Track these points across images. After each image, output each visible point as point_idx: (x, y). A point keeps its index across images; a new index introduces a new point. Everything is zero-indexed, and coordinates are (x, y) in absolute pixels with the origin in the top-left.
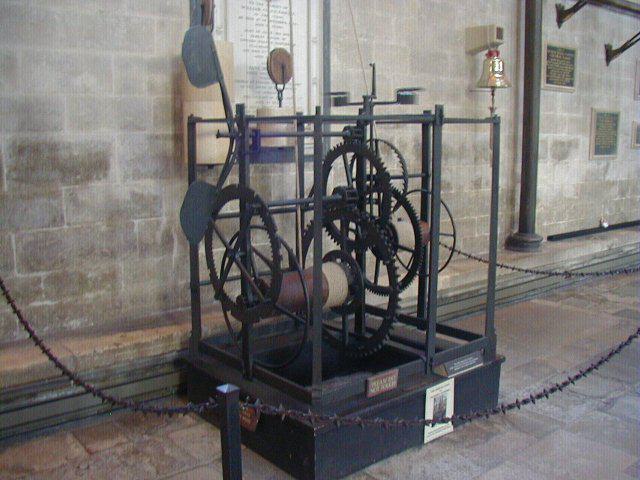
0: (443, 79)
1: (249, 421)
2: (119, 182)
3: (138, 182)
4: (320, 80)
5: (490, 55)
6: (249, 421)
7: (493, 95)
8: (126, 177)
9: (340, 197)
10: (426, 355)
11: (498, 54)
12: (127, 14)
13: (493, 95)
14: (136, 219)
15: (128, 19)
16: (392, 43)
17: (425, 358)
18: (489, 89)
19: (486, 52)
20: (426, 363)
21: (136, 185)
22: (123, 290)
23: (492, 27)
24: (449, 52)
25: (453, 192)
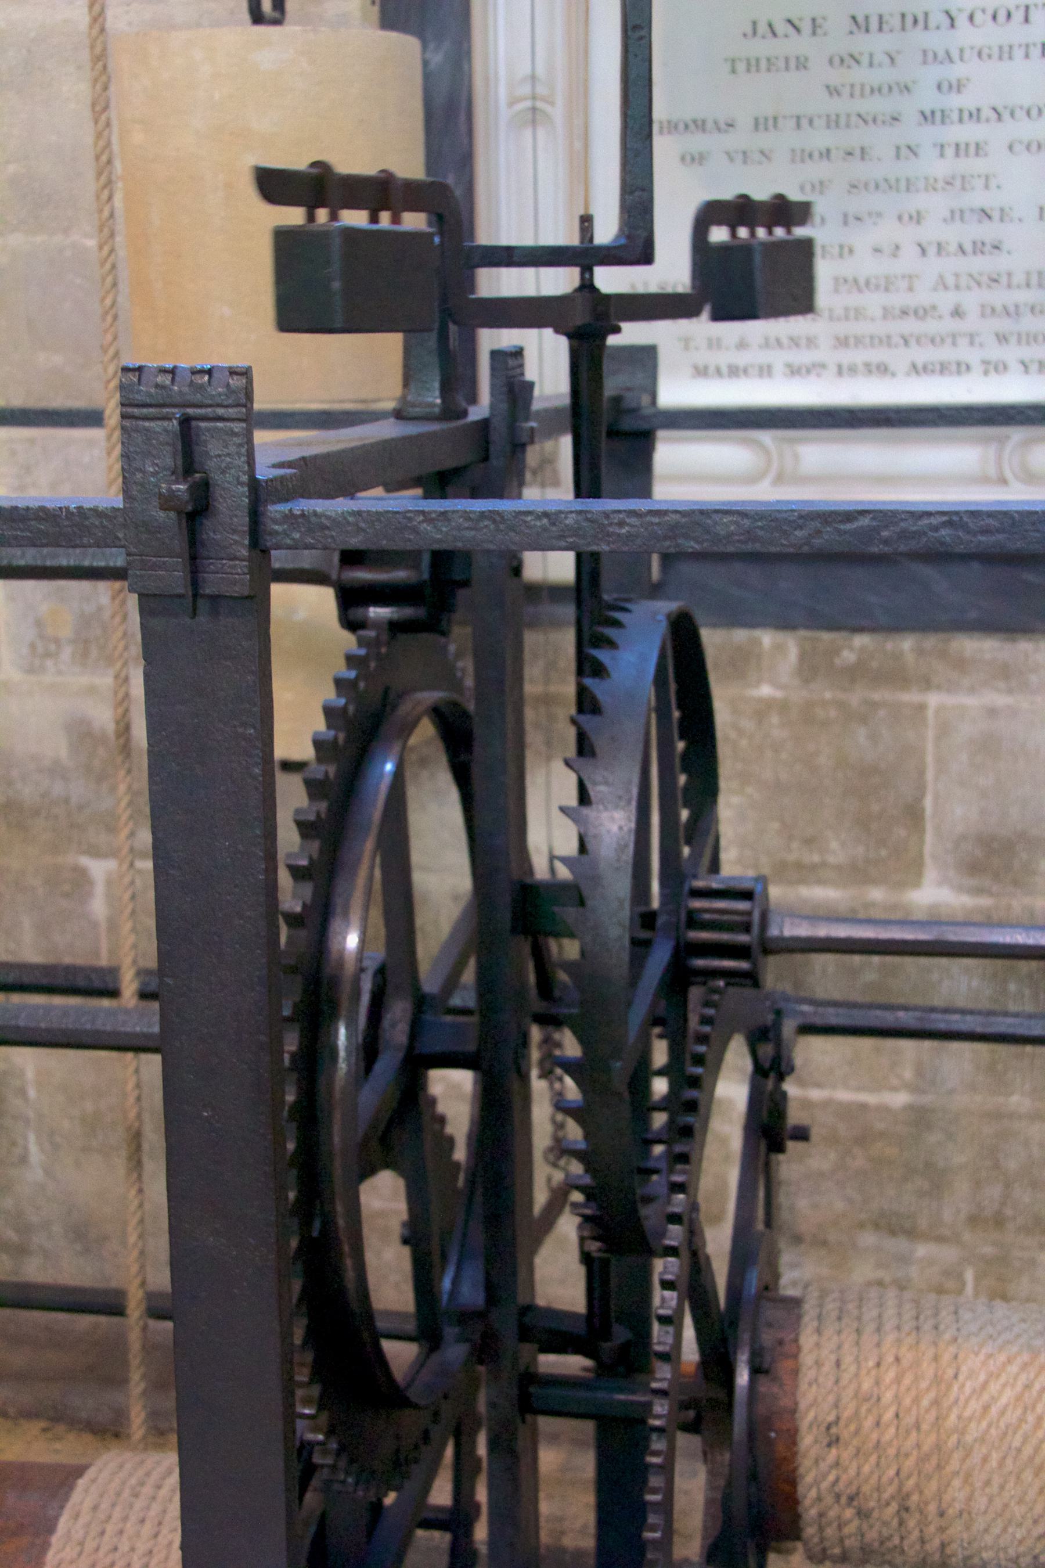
14: (95, 852)
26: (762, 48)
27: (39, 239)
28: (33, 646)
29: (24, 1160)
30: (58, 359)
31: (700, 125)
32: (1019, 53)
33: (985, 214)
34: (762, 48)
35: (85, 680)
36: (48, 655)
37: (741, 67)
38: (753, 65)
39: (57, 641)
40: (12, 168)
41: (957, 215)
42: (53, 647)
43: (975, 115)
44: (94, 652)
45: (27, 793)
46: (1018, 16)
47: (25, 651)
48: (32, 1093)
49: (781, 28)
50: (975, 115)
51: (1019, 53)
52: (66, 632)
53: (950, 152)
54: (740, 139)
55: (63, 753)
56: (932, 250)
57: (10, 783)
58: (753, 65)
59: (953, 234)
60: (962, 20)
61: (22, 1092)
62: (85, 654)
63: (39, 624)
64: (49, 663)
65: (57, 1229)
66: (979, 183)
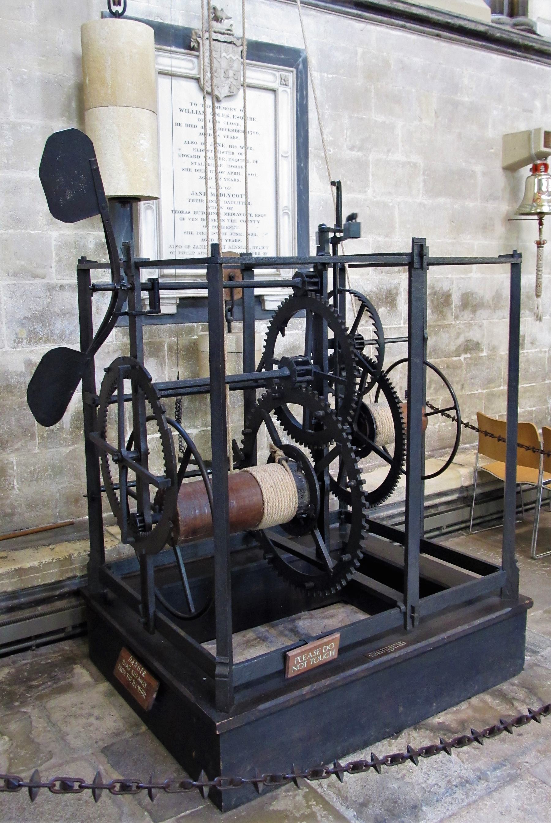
0: (470, 204)
1: (143, 694)
2: (7, 348)
3: (33, 349)
4: (293, 211)
5: (535, 169)
6: (143, 694)
7: (541, 224)
8: (18, 341)
9: (288, 373)
10: (405, 603)
11: (546, 167)
12: (12, 119)
13: (541, 224)
15: (14, 127)
16: (398, 157)
17: (403, 607)
18: (536, 217)
19: (530, 166)
20: (405, 614)
21: (32, 351)
22: (17, 491)
23: (538, 130)
24: (478, 169)
25: (484, 354)
26: (195, 197)
27: (18, 231)
28: (15, 340)
29: (13, 488)
30: (23, 263)
31: (183, 212)
32: (241, 203)
33: (237, 234)
34: (195, 197)
35: (30, 349)
36: (19, 343)
37: (191, 201)
38: (193, 201)
39: (22, 339)
40: (10, 213)
41: (232, 234)
42: (21, 340)
43: (234, 214)
44: (33, 341)
45: (13, 382)
46: (240, 196)
47: (12, 342)
48: (15, 468)
49: (198, 193)
50: (234, 214)
51: (241, 203)
52: (24, 336)
53: (230, 221)
54: (192, 215)
55: (23, 369)
56: (228, 241)
57: (8, 380)
58: (193, 201)
59: (232, 237)
60: (231, 196)
61: (12, 468)
62: (30, 341)
63: (16, 334)
64: (20, 344)
65: (23, 506)
66: (235, 228)
